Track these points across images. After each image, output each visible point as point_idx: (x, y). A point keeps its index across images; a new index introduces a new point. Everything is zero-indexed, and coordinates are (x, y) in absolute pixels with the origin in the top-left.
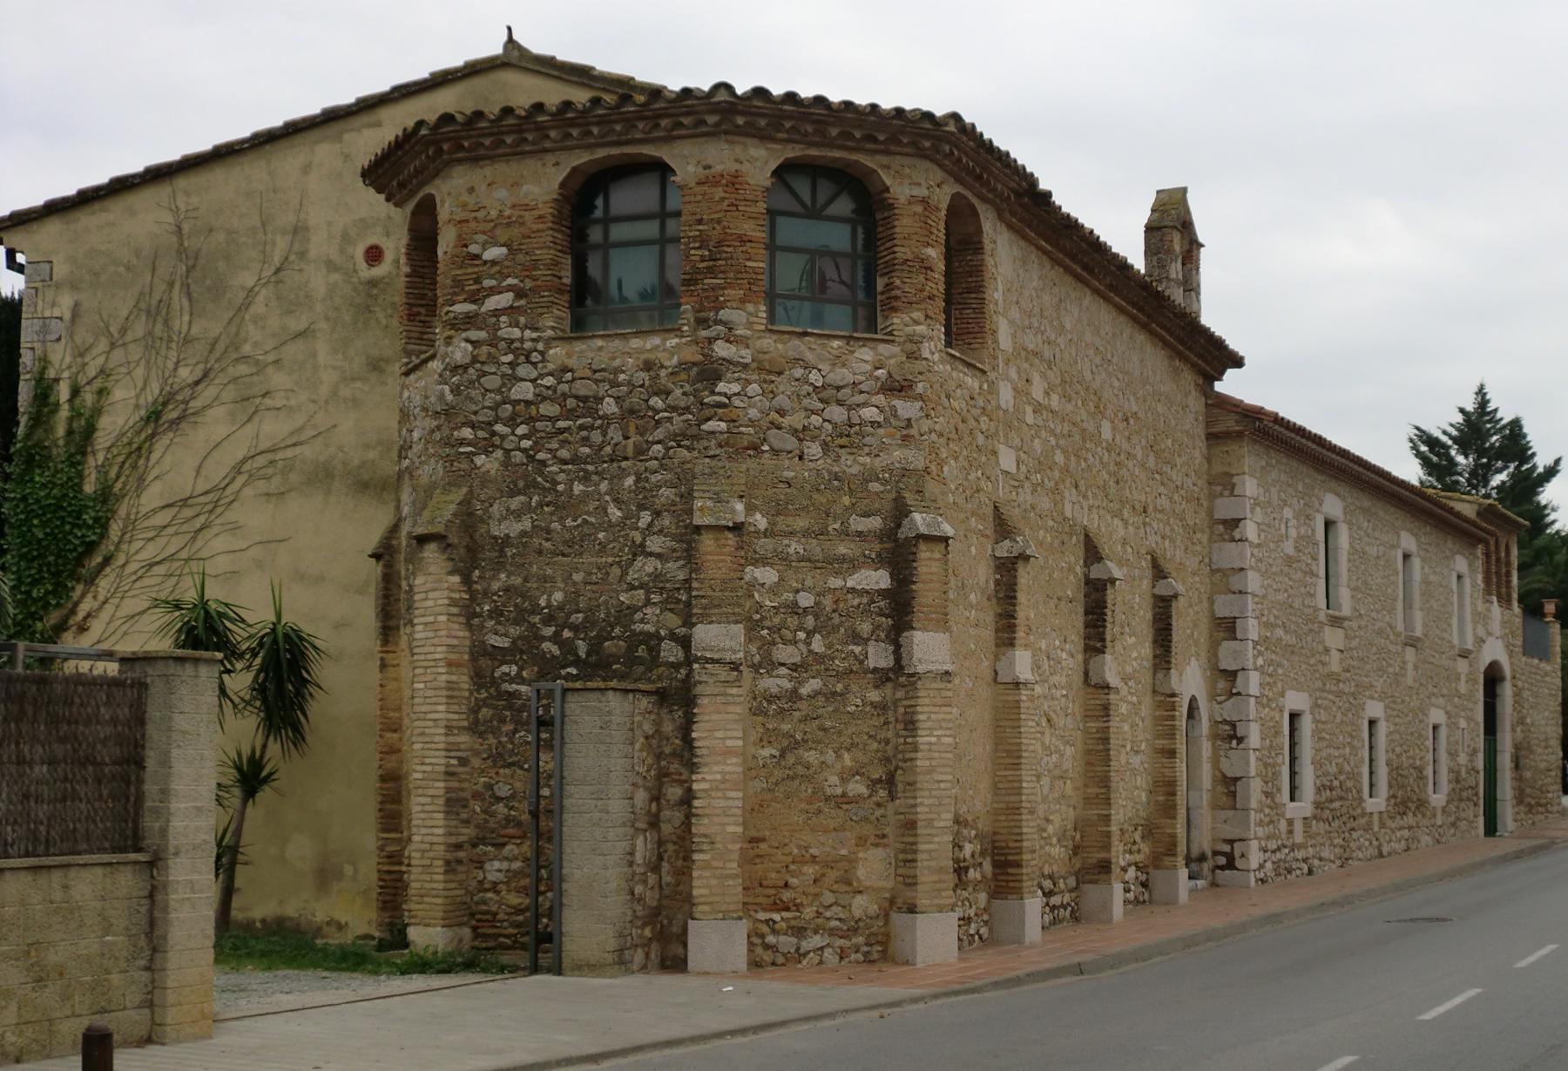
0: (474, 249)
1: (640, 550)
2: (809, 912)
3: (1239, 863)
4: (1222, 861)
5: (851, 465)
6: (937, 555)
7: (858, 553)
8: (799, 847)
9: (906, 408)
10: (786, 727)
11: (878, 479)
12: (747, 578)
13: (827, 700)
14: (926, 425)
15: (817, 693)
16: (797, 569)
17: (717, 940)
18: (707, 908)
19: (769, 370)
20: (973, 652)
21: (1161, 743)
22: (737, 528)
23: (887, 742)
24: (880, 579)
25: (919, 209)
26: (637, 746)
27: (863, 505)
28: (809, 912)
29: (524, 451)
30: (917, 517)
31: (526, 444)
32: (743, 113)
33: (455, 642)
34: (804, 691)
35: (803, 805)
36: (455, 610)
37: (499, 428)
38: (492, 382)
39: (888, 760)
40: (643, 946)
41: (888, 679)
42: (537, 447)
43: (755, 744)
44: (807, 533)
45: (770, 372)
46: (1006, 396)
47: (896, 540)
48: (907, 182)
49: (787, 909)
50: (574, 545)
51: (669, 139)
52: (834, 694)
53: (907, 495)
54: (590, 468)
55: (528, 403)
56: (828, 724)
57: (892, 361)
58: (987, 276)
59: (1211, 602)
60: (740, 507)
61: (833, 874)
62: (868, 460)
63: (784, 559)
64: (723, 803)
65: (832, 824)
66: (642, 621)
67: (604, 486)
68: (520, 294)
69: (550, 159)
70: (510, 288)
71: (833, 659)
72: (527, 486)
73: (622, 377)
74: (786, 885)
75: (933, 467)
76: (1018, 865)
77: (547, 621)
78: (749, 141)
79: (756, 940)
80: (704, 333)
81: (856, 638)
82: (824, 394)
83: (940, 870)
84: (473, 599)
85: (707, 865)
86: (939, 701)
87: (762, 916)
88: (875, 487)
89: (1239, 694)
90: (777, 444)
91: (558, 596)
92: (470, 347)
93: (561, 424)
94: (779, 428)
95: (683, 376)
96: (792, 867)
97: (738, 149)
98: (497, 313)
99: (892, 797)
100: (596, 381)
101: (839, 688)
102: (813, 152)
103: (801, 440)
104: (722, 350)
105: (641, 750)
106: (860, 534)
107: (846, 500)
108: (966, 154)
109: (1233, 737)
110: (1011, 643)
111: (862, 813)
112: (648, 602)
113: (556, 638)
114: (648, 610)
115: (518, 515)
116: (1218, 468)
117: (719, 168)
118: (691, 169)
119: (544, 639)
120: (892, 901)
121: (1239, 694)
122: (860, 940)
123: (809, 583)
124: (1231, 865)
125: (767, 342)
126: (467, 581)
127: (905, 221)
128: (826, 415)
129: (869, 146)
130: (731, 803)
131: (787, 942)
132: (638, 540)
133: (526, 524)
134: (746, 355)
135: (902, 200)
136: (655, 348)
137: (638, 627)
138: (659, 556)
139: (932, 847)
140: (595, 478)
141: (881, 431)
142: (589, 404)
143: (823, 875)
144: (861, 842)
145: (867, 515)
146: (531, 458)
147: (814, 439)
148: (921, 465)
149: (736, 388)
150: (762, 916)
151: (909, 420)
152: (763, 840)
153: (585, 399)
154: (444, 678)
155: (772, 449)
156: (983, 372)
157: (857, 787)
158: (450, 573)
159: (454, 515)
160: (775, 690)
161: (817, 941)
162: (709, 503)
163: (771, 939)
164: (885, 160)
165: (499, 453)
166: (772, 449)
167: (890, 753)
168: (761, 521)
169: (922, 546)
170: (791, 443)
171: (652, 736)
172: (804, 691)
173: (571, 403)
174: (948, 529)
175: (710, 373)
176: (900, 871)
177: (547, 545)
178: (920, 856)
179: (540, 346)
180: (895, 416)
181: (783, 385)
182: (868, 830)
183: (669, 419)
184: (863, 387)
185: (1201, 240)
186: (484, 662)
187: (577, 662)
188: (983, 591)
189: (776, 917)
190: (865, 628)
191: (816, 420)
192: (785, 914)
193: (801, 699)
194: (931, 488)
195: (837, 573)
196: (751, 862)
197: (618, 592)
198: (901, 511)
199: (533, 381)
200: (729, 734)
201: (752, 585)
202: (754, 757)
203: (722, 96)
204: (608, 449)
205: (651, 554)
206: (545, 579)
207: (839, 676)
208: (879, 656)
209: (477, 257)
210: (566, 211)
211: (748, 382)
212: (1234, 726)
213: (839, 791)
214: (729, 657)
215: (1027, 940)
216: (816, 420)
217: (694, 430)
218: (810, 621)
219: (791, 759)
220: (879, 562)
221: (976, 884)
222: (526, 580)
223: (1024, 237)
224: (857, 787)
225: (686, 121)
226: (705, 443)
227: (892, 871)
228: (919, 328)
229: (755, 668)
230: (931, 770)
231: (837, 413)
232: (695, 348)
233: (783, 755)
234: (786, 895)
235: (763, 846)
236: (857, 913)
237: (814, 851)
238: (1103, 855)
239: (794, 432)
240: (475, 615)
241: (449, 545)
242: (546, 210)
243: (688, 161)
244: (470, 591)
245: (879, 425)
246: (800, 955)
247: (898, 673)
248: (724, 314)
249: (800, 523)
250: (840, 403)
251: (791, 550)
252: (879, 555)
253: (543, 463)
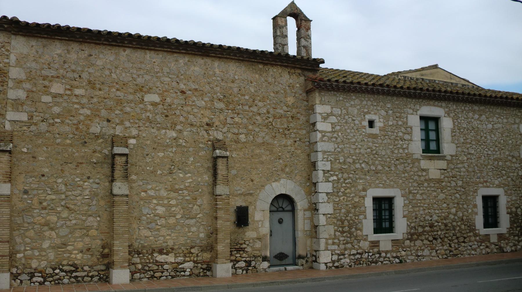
4: (314, 258)
59: (309, 155)
89: (316, 192)
121: (316, 192)
124: (315, 261)
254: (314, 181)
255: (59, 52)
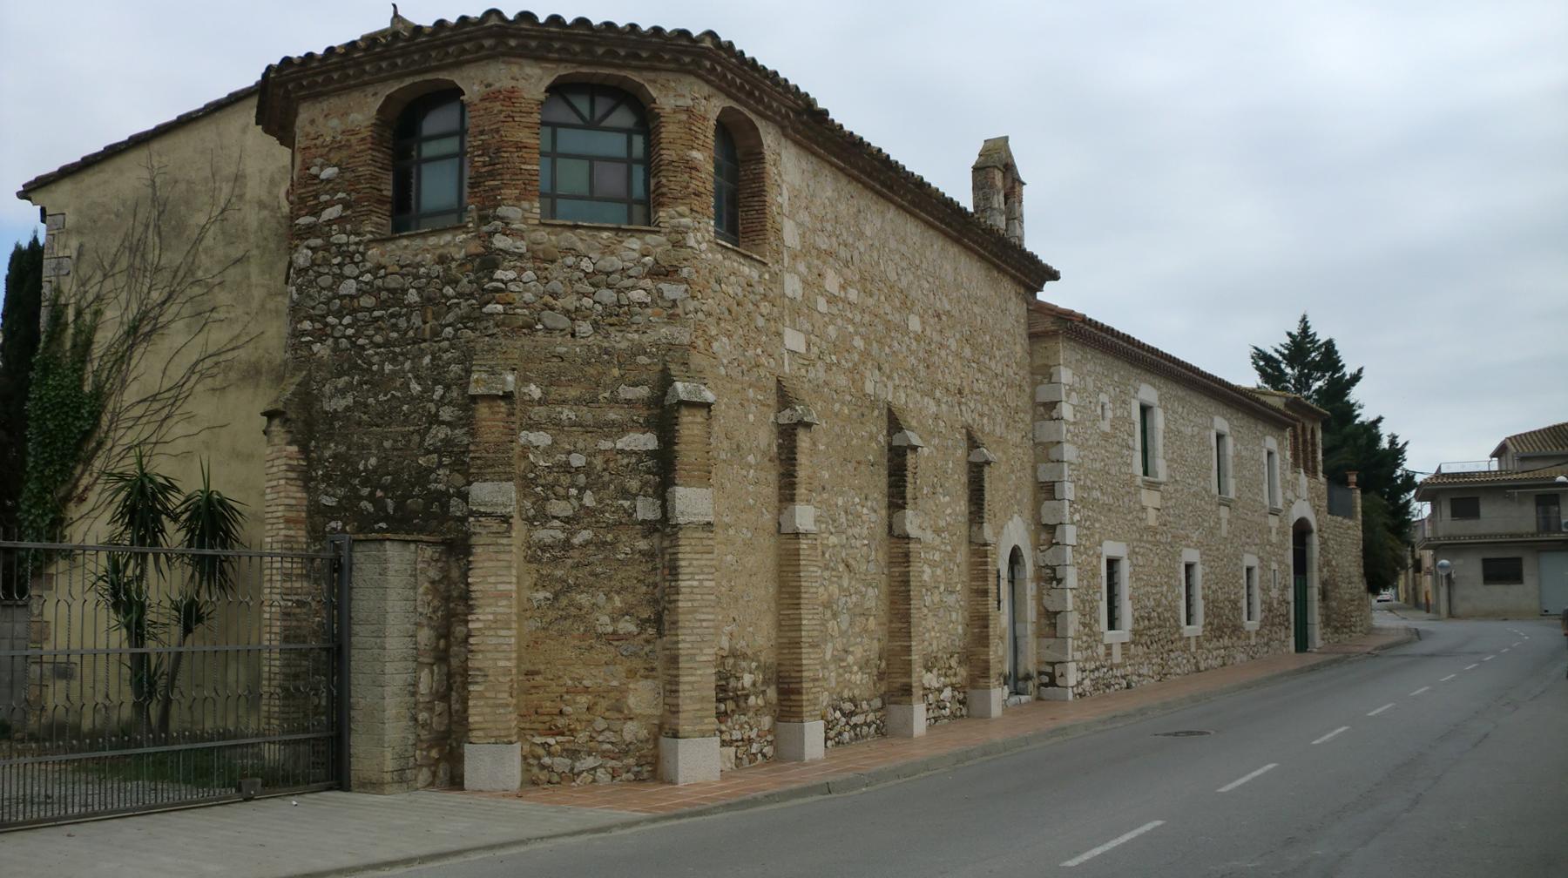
0: (314, 170)
1: (435, 419)
2: (582, 737)
3: (1058, 681)
4: (1046, 679)
5: (621, 341)
6: (699, 419)
7: (626, 418)
8: (572, 679)
9: (671, 290)
10: (559, 573)
11: (645, 353)
12: (522, 441)
13: (598, 548)
14: (691, 305)
15: (587, 543)
16: (569, 434)
17: (493, 764)
18: (480, 733)
19: (542, 259)
20: (751, 507)
21: (975, 584)
22: (508, 397)
23: (655, 585)
24: (649, 441)
25: (684, 117)
26: (421, 590)
27: (631, 376)
28: (582, 737)
29: (349, 338)
30: (679, 385)
31: (350, 332)
32: (513, 36)
33: (293, 502)
34: (576, 541)
35: (576, 642)
36: (292, 475)
37: (330, 319)
38: (325, 281)
39: (656, 602)
40: (429, 766)
41: (656, 530)
42: (357, 335)
43: (529, 588)
44: (578, 401)
45: (544, 261)
46: (793, 286)
47: (663, 407)
48: (671, 94)
49: (562, 734)
50: (386, 415)
51: (458, 65)
52: (605, 543)
53: (672, 366)
54: (398, 350)
55: (352, 297)
56: (599, 570)
57: (659, 250)
58: (768, 182)
60: (510, 378)
61: (604, 703)
62: (636, 336)
63: (557, 425)
64: (494, 641)
65: (604, 658)
66: (435, 481)
67: (408, 365)
68: (346, 205)
69: (370, 90)
70: (340, 201)
71: (603, 512)
72: (350, 368)
73: (422, 270)
74: (561, 713)
75: (700, 342)
76: (799, 692)
77: (364, 484)
78: (523, 61)
79: (531, 761)
80: (485, 228)
81: (625, 493)
82: (596, 279)
83: (702, 699)
84: (310, 465)
85: (481, 696)
86: (700, 548)
87: (538, 740)
88: (643, 360)
90: (549, 323)
91: (373, 461)
92: (310, 253)
93: (376, 314)
94: (552, 309)
95: (469, 267)
96: (566, 697)
97: (515, 69)
98: (329, 223)
99: (660, 634)
100: (403, 276)
101: (610, 537)
102: (584, 70)
103: (573, 320)
104: (500, 242)
105: (426, 594)
106: (628, 401)
107: (616, 372)
108: (731, 70)
109: (1054, 578)
110: (791, 499)
111: (632, 649)
112: (440, 465)
113: (371, 498)
114: (441, 472)
115: (342, 392)
116: (1038, 362)
117: (497, 86)
118: (476, 88)
119: (362, 498)
120: (661, 727)
122: (631, 761)
123: (580, 445)
124: (1052, 683)
125: (542, 235)
126: (305, 450)
127: (671, 128)
128: (597, 298)
129: (634, 63)
130: (501, 640)
131: (561, 763)
132: (433, 410)
133: (349, 400)
134: (522, 246)
135: (668, 109)
136: (447, 244)
137: (433, 486)
138: (449, 424)
139: (693, 679)
140: (401, 358)
141: (649, 311)
142: (398, 294)
143: (596, 704)
144: (632, 674)
145: (635, 385)
146: (354, 344)
147: (585, 318)
148: (686, 339)
149: (511, 275)
150: (538, 740)
151: (674, 301)
152: (538, 673)
153: (392, 291)
154: (283, 532)
155: (546, 327)
156: (765, 264)
157: (627, 626)
158: (289, 444)
159: (293, 394)
160: (548, 541)
161: (590, 762)
162: (484, 376)
163: (547, 760)
164: (652, 75)
165: (330, 341)
166: (546, 327)
167: (658, 595)
168: (535, 391)
169: (684, 411)
170: (564, 322)
171: (440, 581)
172: (576, 541)
173: (384, 295)
174: (709, 396)
175: (488, 261)
176: (668, 700)
177: (365, 417)
178: (681, 688)
179: (361, 249)
180: (661, 296)
181: (555, 271)
182: (637, 664)
183: (458, 305)
184: (631, 273)
185: (1023, 179)
186: (318, 519)
187: (386, 518)
188: (764, 454)
189: (551, 741)
190: (634, 484)
191: (587, 302)
192: (559, 738)
193: (572, 547)
194: (696, 359)
195: (607, 437)
196: (527, 692)
197: (417, 457)
198: (666, 381)
199: (356, 278)
200: (500, 579)
201: (527, 448)
202: (529, 600)
203: (493, 21)
204: (411, 333)
205: (443, 423)
206: (364, 447)
207: (609, 527)
208: (646, 510)
209: (317, 177)
210: (388, 134)
211: (524, 269)
212: (1053, 569)
213: (610, 629)
214: (500, 510)
215: (807, 758)
216: (587, 302)
217: (477, 314)
218: (582, 479)
219: (564, 602)
220: (647, 426)
221: (758, 711)
222: (349, 448)
223: (814, 153)
224: (627, 626)
225: (467, 46)
226: (485, 324)
227: (661, 699)
228: (684, 221)
229: (530, 521)
230: (694, 610)
231: (607, 296)
232: (478, 242)
233: (556, 597)
234: (561, 722)
235: (538, 678)
236: (628, 737)
237: (586, 683)
238: (905, 680)
239: (567, 312)
240: (313, 479)
241: (288, 420)
242: (366, 133)
243: (471, 82)
244: (307, 458)
245: (647, 305)
246: (574, 774)
247: (664, 526)
248: (502, 211)
249: (573, 393)
250: (609, 286)
251: (564, 417)
252: (647, 420)
253: (362, 347)
254: (1048, 519)
255: (829, 194)
